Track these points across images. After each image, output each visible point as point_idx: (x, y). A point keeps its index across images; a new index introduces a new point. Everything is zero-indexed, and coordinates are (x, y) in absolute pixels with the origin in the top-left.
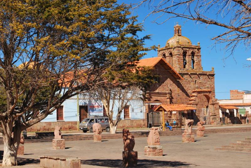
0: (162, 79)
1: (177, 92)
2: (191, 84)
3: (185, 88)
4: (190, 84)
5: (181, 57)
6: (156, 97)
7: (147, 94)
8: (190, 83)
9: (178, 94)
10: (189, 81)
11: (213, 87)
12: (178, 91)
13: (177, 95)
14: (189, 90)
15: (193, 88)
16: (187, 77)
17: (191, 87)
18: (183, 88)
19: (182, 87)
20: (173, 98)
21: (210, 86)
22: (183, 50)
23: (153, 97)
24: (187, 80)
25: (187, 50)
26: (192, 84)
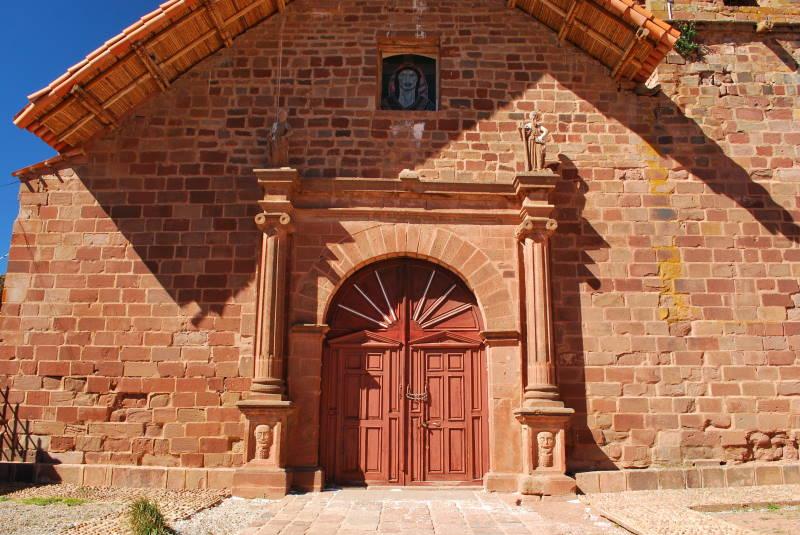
0: (468, 74)
1: (644, 188)
3: (732, 151)
6: (386, 227)
7: (273, 193)
8: (781, 102)
9: (660, 200)
10: (768, 90)
12: (661, 177)
13: (646, 211)
16: (743, 59)
18: (715, 150)
19: (703, 138)
20: (598, 242)
23: (362, 224)
24: (743, 77)
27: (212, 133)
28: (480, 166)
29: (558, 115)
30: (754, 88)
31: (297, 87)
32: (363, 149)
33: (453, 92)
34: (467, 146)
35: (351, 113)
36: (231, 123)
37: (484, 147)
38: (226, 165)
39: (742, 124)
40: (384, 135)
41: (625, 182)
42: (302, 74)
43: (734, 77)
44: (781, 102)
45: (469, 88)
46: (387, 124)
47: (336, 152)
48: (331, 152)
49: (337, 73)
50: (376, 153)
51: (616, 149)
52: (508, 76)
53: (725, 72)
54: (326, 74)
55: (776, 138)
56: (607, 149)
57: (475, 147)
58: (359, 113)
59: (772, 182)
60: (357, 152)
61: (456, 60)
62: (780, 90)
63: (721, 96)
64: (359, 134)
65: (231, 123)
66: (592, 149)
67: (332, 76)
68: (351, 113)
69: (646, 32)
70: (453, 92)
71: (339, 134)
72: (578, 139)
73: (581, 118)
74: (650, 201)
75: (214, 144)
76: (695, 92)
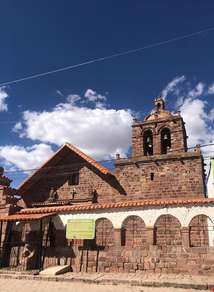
2: (141, 180)
4: (139, 180)
5: (139, 140)
10: (136, 175)
11: (197, 182)
14: (138, 191)
15: (147, 188)
16: (131, 169)
17: (140, 186)
21: (189, 180)
22: (142, 128)
24: (131, 173)
25: (150, 128)
26: (144, 180)
27: (43, 192)
28: (84, 195)
29: (97, 184)
30: (133, 176)
31: (56, 182)
32: (66, 193)
33: (81, 181)
34: (82, 192)
35: (64, 187)
36: (46, 190)
37: (85, 192)
38: (45, 197)
39: (130, 183)
40: (69, 191)
41: (108, 197)
42: (57, 180)
43: (129, 173)
44: (138, 178)
45: (83, 180)
46: (70, 189)
47: (62, 194)
48: (61, 194)
49: (63, 179)
50: (68, 194)
51: (107, 190)
52: (89, 177)
53: (128, 172)
54: (60, 180)
55: (136, 186)
56: (105, 190)
57: (83, 192)
58: (66, 187)
59: (135, 195)
60: (65, 194)
61: (82, 175)
62: (138, 175)
63: (127, 178)
64: (65, 191)
65: (46, 190)
66: (102, 191)
67: (62, 180)
68: (64, 187)
69: (102, 173)
70: (81, 181)
71: (62, 191)
72: (100, 189)
73: (101, 185)
74: (112, 200)
75: (43, 194)
76: (122, 177)
